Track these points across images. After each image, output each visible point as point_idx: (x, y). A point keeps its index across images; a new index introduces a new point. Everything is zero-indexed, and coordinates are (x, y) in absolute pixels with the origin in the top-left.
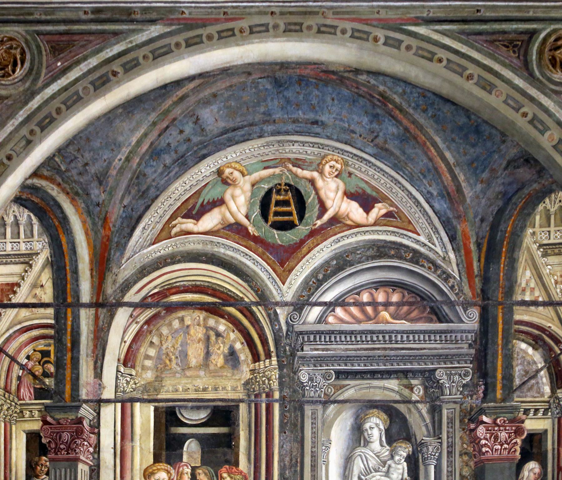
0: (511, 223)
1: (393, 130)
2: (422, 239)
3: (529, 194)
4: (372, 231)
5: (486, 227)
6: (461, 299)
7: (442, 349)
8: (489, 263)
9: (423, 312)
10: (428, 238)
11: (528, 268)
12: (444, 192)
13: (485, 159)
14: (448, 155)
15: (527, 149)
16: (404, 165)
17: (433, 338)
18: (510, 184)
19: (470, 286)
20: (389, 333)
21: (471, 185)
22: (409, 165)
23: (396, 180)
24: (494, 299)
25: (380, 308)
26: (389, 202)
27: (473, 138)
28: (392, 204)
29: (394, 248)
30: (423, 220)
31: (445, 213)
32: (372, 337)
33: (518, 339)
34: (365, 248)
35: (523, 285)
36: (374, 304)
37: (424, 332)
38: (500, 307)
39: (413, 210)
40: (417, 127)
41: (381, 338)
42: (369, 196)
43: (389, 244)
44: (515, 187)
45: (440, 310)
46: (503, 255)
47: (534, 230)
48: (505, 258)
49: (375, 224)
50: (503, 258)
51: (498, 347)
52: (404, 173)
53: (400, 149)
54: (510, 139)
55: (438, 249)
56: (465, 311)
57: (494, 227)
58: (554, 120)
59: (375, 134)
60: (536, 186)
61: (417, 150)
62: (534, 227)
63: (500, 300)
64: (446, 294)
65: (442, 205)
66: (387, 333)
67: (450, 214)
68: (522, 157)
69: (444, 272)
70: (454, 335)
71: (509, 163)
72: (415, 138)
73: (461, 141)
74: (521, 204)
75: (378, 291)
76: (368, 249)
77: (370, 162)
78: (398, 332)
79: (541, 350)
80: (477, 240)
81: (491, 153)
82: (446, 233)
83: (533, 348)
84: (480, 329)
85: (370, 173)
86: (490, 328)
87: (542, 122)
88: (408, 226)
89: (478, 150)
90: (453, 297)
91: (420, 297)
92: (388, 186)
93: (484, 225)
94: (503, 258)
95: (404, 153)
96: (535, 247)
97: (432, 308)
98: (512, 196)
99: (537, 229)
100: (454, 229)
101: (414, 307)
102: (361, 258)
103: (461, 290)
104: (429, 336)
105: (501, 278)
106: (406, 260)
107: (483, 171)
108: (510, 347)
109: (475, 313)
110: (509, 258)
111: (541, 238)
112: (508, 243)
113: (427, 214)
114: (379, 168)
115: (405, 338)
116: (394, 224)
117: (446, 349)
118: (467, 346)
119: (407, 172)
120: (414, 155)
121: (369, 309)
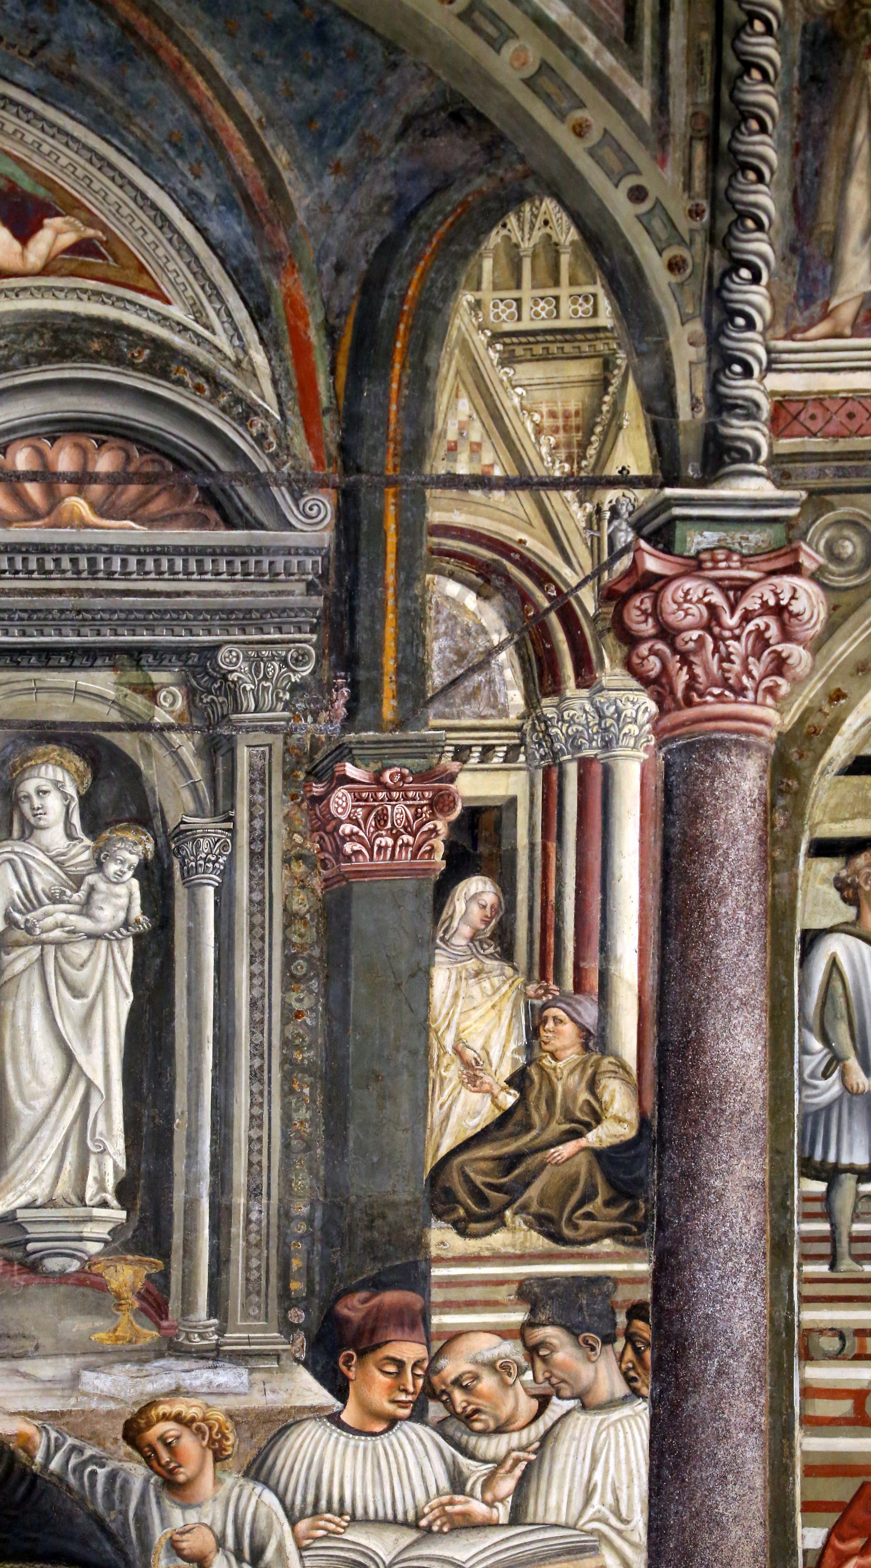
0: (417, 276)
1: (90, 26)
2: (176, 312)
3: (464, 203)
4: (38, 288)
5: (350, 286)
6: (285, 469)
7: (234, 594)
8: (360, 379)
9: (183, 501)
10: (192, 308)
11: (463, 392)
12: (236, 195)
13: (342, 112)
14: (243, 97)
15: (457, 87)
16: (122, 120)
17: (209, 566)
18: (413, 176)
19: (309, 437)
20: (89, 551)
21: (307, 177)
22: (138, 120)
23: (102, 158)
24: (373, 469)
25: (65, 487)
26: (83, 215)
27: (310, 54)
28: (92, 221)
29: (99, 335)
30: (177, 264)
31: (239, 249)
32: (41, 563)
33: (440, 572)
34: (18, 332)
35: (452, 435)
36: (46, 476)
37: (186, 551)
38: (391, 490)
39: (150, 238)
40: (156, 22)
41: (66, 564)
42: (27, 197)
43: (86, 325)
44: (426, 184)
45: (229, 498)
46: (398, 358)
47: (479, 295)
48: (403, 367)
49: (45, 271)
50: (397, 366)
51: (385, 592)
52: (124, 141)
53: (111, 79)
54: (410, 58)
55: (222, 340)
56: (296, 501)
57: (372, 286)
58: (526, 12)
59: (41, 36)
60: (480, 182)
61: (159, 82)
62: (478, 288)
63: (390, 472)
64: (245, 455)
65: (229, 227)
66: (83, 551)
67: (251, 251)
68: (443, 108)
69: (238, 400)
70: (266, 561)
71: (408, 122)
72: (153, 51)
73: (279, 62)
74: (443, 229)
75: (58, 443)
76: (29, 335)
77: (28, 110)
78: (112, 550)
79: (498, 599)
80: (326, 320)
81: (359, 94)
82: (243, 298)
83: (479, 595)
84: (338, 545)
85: (29, 138)
86: (363, 544)
87: (494, 18)
88: (136, 277)
89: (325, 87)
90: (263, 464)
91: (175, 461)
92: (80, 172)
93: (345, 280)
94: (397, 366)
95: (124, 90)
96: (481, 339)
97: (206, 491)
98: (418, 209)
99: (487, 294)
100: (264, 289)
101: (156, 488)
102: (9, 357)
103: (285, 447)
104: (200, 563)
105: (392, 417)
106: (133, 366)
107: (340, 142)
108: (417, 591)
109: (323, 505)
110: (413, 367)
111: (497, 317)
112: (410, 329)
113: (189, 248)
114: (52, 125)
115: (133, 565)
116: (98, 272)
117: (244, 594)
118: (302, 586)
119: (131, 139)
120: (149, 96)
121: (33, 490)
